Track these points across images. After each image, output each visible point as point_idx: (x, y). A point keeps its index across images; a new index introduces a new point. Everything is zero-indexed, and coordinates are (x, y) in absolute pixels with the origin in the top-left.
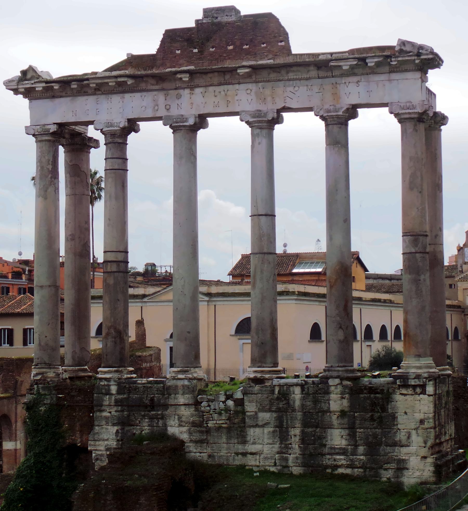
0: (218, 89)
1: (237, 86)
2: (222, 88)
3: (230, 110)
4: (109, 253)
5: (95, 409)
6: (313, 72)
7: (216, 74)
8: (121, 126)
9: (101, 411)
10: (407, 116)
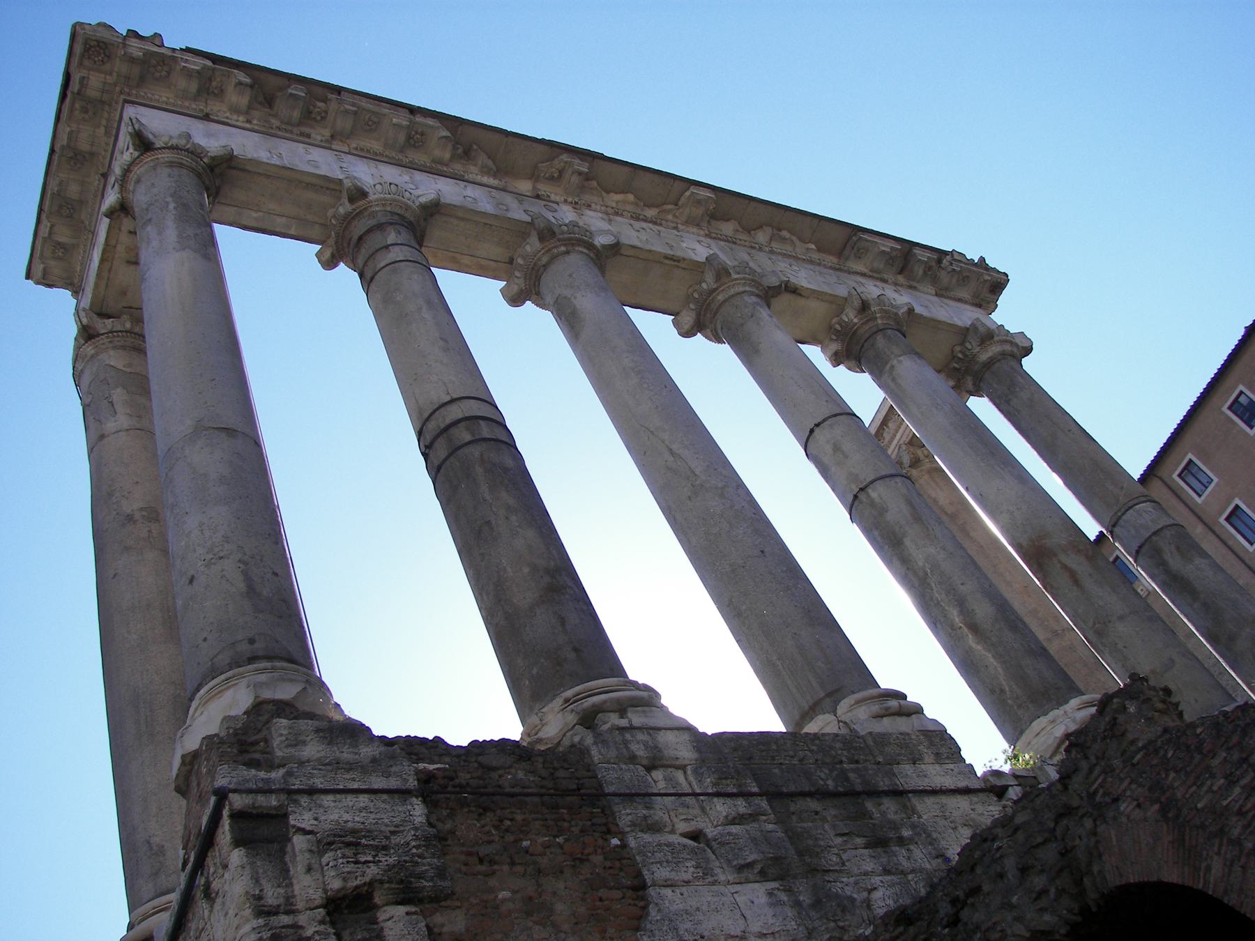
0: (638, 225)
1: (675, 232)
2: (644, 225)
3: (679, 254)
4: (472, 401)
5: (626, 815)
6: (816, 256)
7: (631, 197)
8: (423, 200)
9: (655, 828)
10: (1007, 348)
